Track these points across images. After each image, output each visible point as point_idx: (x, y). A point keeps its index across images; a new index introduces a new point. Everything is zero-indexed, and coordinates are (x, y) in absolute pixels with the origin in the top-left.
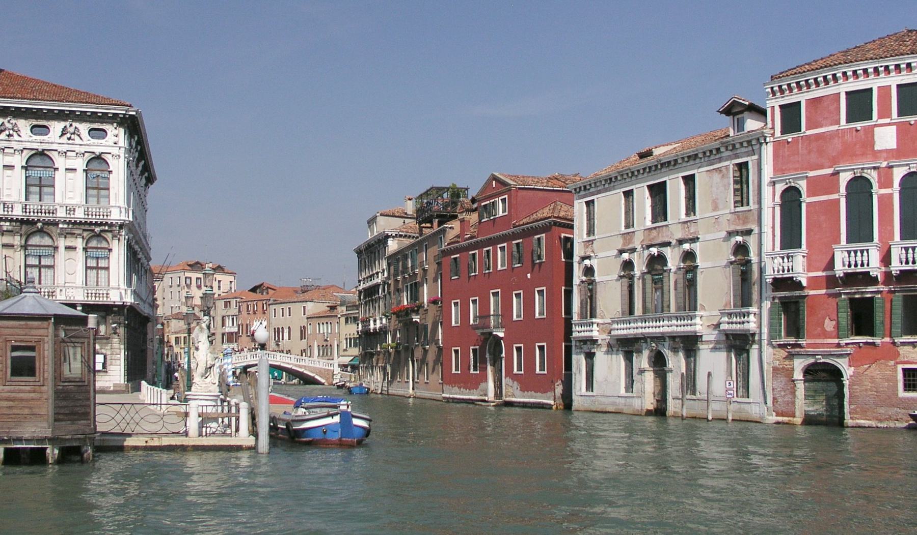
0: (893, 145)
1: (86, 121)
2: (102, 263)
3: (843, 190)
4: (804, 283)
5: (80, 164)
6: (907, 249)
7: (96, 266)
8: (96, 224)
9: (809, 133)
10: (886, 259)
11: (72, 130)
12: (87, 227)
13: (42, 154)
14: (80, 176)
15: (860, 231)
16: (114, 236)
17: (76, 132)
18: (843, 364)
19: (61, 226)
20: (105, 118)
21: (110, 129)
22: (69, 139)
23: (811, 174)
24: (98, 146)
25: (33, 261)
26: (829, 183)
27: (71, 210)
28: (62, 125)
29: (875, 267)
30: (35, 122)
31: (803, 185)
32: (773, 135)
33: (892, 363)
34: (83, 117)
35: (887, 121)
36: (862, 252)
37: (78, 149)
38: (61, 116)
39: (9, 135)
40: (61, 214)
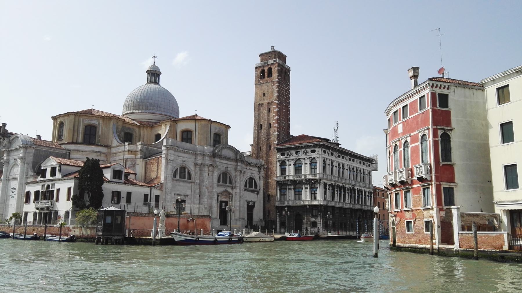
8: (314, 180)
13: (299, 159)
14: (308, 166)
17: (307, 152)
20: (314, 146)
24: (313, 155)
27: (305, 175)
28: (303, 150)
34: (308, 147)
38: (302, 147)
40: (303, 177)
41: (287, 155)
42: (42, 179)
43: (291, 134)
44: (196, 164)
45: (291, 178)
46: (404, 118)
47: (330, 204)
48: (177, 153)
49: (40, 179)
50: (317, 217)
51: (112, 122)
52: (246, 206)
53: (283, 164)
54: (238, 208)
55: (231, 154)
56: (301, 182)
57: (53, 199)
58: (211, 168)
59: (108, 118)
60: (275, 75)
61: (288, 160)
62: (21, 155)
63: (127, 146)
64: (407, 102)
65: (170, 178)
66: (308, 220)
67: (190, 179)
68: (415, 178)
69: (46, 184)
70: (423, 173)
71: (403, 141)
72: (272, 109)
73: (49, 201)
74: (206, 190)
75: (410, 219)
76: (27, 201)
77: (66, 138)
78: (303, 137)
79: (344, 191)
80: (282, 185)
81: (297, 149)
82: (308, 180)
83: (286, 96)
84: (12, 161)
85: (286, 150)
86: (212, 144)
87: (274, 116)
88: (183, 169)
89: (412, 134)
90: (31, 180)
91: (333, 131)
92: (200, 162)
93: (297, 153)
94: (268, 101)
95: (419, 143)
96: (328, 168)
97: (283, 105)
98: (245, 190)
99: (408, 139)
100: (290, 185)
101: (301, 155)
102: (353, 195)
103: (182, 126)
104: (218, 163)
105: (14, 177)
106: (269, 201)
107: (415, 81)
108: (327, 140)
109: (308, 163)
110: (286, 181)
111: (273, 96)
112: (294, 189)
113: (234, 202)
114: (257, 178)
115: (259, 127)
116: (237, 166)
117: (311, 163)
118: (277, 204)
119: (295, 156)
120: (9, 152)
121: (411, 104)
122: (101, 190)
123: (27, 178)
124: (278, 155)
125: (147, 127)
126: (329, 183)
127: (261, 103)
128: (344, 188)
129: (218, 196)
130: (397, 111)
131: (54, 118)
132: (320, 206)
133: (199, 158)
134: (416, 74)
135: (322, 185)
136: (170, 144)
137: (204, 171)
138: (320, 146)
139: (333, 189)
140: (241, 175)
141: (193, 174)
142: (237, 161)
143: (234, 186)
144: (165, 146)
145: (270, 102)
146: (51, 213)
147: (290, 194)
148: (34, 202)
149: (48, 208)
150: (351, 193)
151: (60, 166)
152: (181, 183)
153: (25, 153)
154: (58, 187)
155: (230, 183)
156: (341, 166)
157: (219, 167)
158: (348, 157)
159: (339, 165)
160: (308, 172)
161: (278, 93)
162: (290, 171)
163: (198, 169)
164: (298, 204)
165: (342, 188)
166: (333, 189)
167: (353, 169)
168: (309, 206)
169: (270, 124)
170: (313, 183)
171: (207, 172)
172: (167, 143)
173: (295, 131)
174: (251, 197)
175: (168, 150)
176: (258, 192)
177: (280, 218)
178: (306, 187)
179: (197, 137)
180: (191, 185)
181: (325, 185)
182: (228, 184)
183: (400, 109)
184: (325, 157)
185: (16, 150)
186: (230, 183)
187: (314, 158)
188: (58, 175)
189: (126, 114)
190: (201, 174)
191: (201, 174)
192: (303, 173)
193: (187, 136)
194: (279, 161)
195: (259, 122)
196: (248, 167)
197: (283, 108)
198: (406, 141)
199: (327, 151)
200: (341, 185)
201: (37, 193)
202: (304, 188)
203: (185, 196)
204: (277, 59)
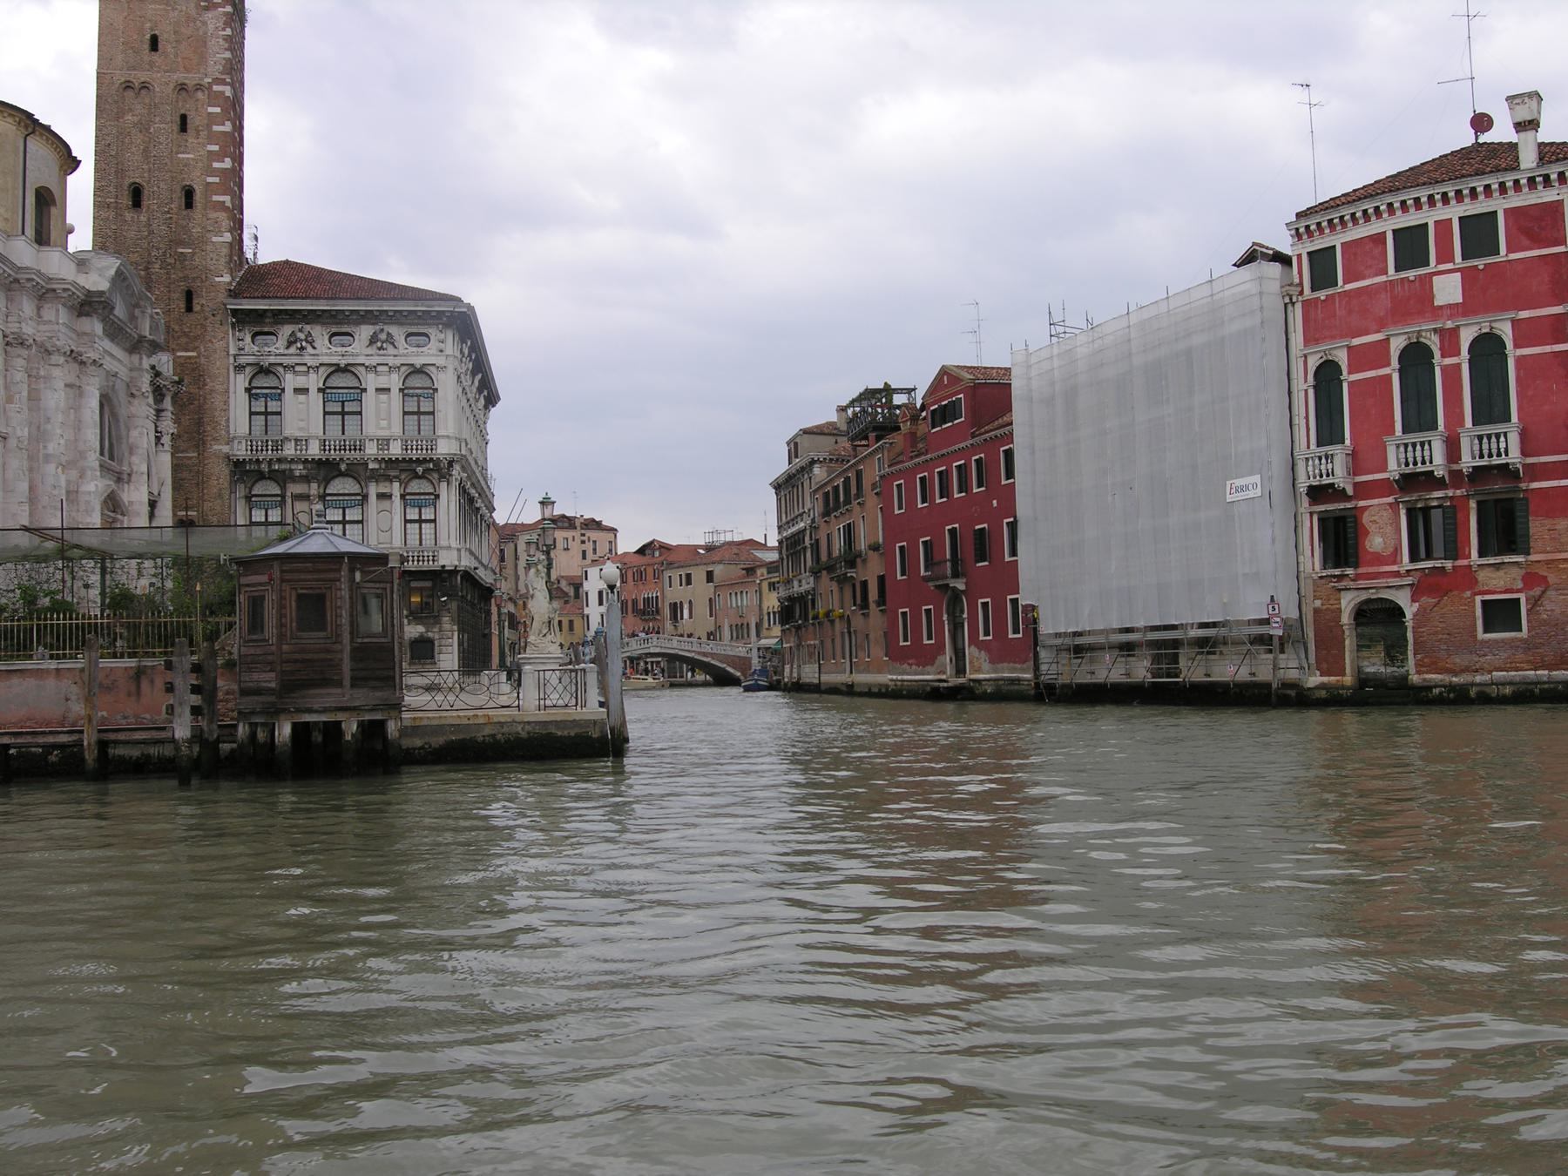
0: (1457, 297)
1: (402, 324)
2: (427, 514)
3: (1395, 363)
4: (1350, 492)
5: (395, 381)
6: (1480, 438)
9: (1349, 287)
10: (1453, 452)
11: (383, 336)
15: (1419, 417)
16: (442, 477)
17: (390, 339)
18: (1403, 599)
19: (371, 466)
22: (381, 348)
23: (1356, 341)
26: (1378, 354)
27: (384, 443)
29: (1438, 462)
30: (334, 330)
31: (1342, 358)
32: (1301, 293)
33: (1468, 593)
35: (1450, 266)
36: (1422, 444)
37: (391, 361)
39: (302, 348)
40: (371, 449)
41: (290, 344)
45: (314, 450)
50: (437, 620)
56: (357, 471)
72: (195, 121)
85: (283, 323)
94: (179, 76)
100: (306, 479)
101: (359, 348)
110: (279, 461)
111: (203, 59)
112: (322, 497)
127: (139, 77)
135: (455, 484)
160: (397, 430)
169: (189, 194)
191: (34, 397)
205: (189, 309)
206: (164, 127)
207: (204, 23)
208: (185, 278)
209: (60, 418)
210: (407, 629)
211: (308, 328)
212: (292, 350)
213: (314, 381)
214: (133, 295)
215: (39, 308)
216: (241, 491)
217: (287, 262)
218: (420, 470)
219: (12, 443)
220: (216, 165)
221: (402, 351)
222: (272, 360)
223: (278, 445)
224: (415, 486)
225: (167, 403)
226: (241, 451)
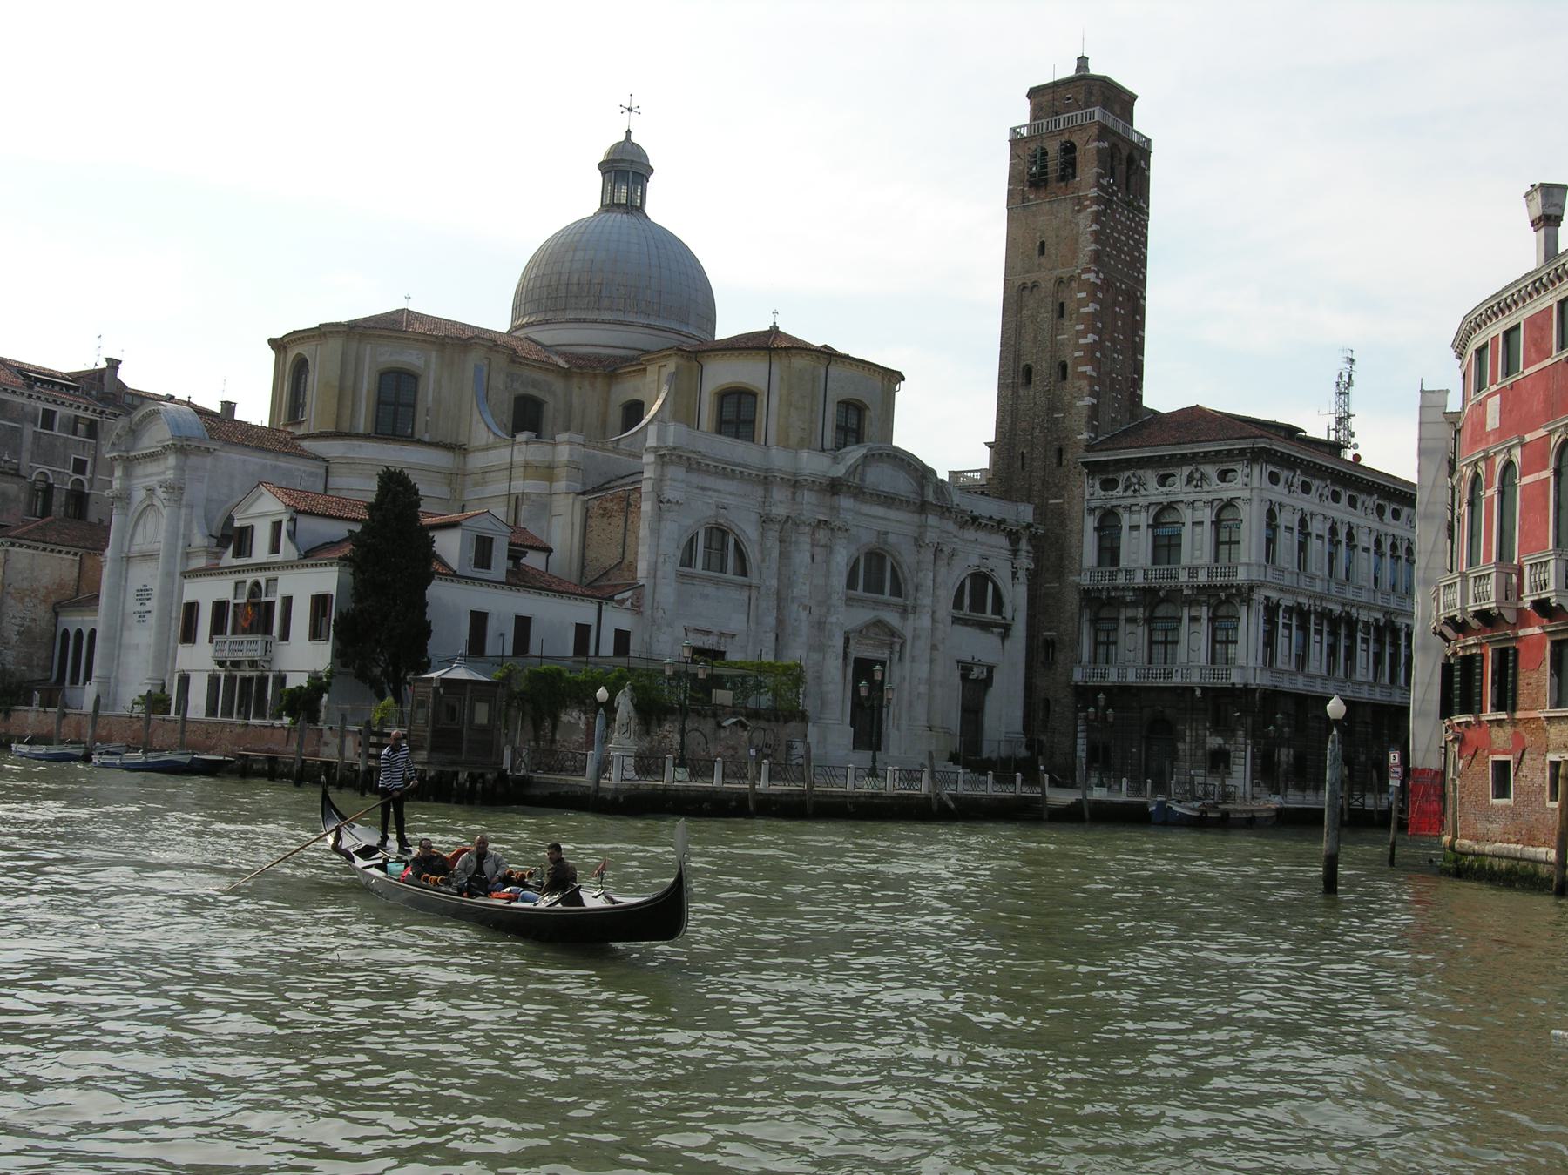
5: (1207, 515)
7: (1221, 640)
11: (1197, 475)
12: (1212, 592)
13: (1171, 506)
14: (1207, 532)
16: (1243, 601)
17: (1203, 478)
20: (1230, 455)
21: (1241, 469)
24: (1226, 492)
25: (1159, 636)
27: (1193, 572)
28: (1186, 470)
34: (1207, 458)
37: (1205, 497)
38: (1184, 459)
41: (1126, 489)
42: (236, 562)
43: (1148, 402)
44: (765, 520)
45: (1139, 579)
46: (1507, 374)
47: (1286, 684)
48: (695, 479)
49: (228, 559)
51: (475, 358)
52: (957, 680)
53: (1108, 523)
54: (923, 689)
55: (902, 484)
56: (1174, 596)
57: (267, 630)
58: (822, 535)
59: (456, 342)
60: (1088, 171)
61: (1128, 508)
62: (170, 475)
63: (525, 449)
64: (1520, 316)
65: (670, 568)
66: (1200, 742)
67: (744, 573)
68: (1526, 603)
69: (250, 578)
70: (1552, 586)
71: (1499, 462)
72: (1070, 306)
73: (259, 638)
74: (804, 615)
75: (1505, 752)
76: (189, 635)
77: (316, 414)
78: (1194, 420)
79: (1351, 636)
80: (1102, 606)
81: (1164, 467)
82: (1201, 589)
83: (1130, 254)
84: (139, 495)
85: (1123, 470)
86: (828, 444)
87: (1083, 334)
88: (718, 534)
89: (1528, 438)
90: (200, 562)
91: (1334, 389)
92: (780, 511)
93: (1163, 480)
94: (1058, 273)
95: (1548, 474)
96: (1287, 543)
97: (1119, 291)
98: (956, 620)
99: (1517, 454)
100: (1134, 604)
101: (1179, 489)
102: (1388, 650)
103: (720, 374)
104: (849, 517)
105: (147, 548)
106: (1050, 663)
107: (1546, 236)
108: (1291, 432)
109: (1207, 524)
110: (1116, 588)
111: (1075, 253)
112: (1149, 620)
113: (907, 664)
114: (1002, 574)
115: (1018, 375)
116: (923, 527)
117: (1217, 524)
118: (1078, 676)
119: (1154, 493)
120: (129, 462)
121: (1530, 321)
122: (419, 604)
123: (187, 556)
124: (1090, 492)
125: (595, 376)
126: (1287, 601)
127: (1034, 277)
128: (1352, 624)
129: (847, 640)
130: (1485, 346)
131: (274, 343)
132: (1247, 690)
133: (779, 494)
134: (1553, 211)
136: (671, 442)
137: (796, 543)
138: (1256, 456)
139: (1303, 627)
140: (940, 563)
141: (753, 555)
142: (923, 507)
143: (910, 602)
144: (655, 450)
145: (1065, 276)
146: (263, 680)
147: (1132, 640)
148: (211, 641)
149: (253, 664)
150: (1380, 641)
151: (293, 520)
152: (710, 590)
153: (180, 469)
154: (287, 593)
155: (897, 590)
156: (1342, 536)
157: (854, 531)
158: (1372, 501)
159: (1333, 531)
161: (1096, 241)
162: (1136, 549)
163: (773, 534)
164: (1161, 682)
165: (1341, 625)
166: (1303, 627)
167: (1394, 547)
168: (1204, 689)
169: (1064, 366)
170: (1222, 600)
171: (808, 547)
172: (661, 436)
173: (1165, 389)
174: (979, 646)
175: (663, 464)
176: (1006, 630)
177: (1090, 729)
178: (1194, 613)
179: (771, 414)
180: (745, 594)
181: (1271, 610)
182: (887, 596)
183: (1495, 339)
184: (1275, 498)
185: (152, 457)
186: (897, 590)
187: (1230, 504)
188: (287, 550)
189: (523, 326)
190: (784, 556)
191: (784, 556)
192: (1185, 559)
193: (737, 412)
194: (1092, 511)
195: (1017, 358)
196: (970, 534)
197: (1115, 303)
198: (1509, 464)
199: (1284, 474)
200: (1337, 609)
201: (220, 608)
202: (1186, 620)
203: (722, 634)
204: (1097, 109)
205: (1060, 463)
206: (1046, 316)
207: (1077, 224)
208: (1058, 438)
209: (803, 571)
210: (1209, 740)
211: (1140, 472)
212: (1130, 493)
213: (1144, 519)
214: (916, 469)
215: (794, 494)
216: (1086, 615)
217: (1196, 410)
218: (1222, 595)
219: (763, 590)
220: (1082, 341)
221: (1214, 487)
222: (1114, 502)
223: (1112, 576)
224: (1222, 611)
225: (1024, 545)
226: (1085, 581)
